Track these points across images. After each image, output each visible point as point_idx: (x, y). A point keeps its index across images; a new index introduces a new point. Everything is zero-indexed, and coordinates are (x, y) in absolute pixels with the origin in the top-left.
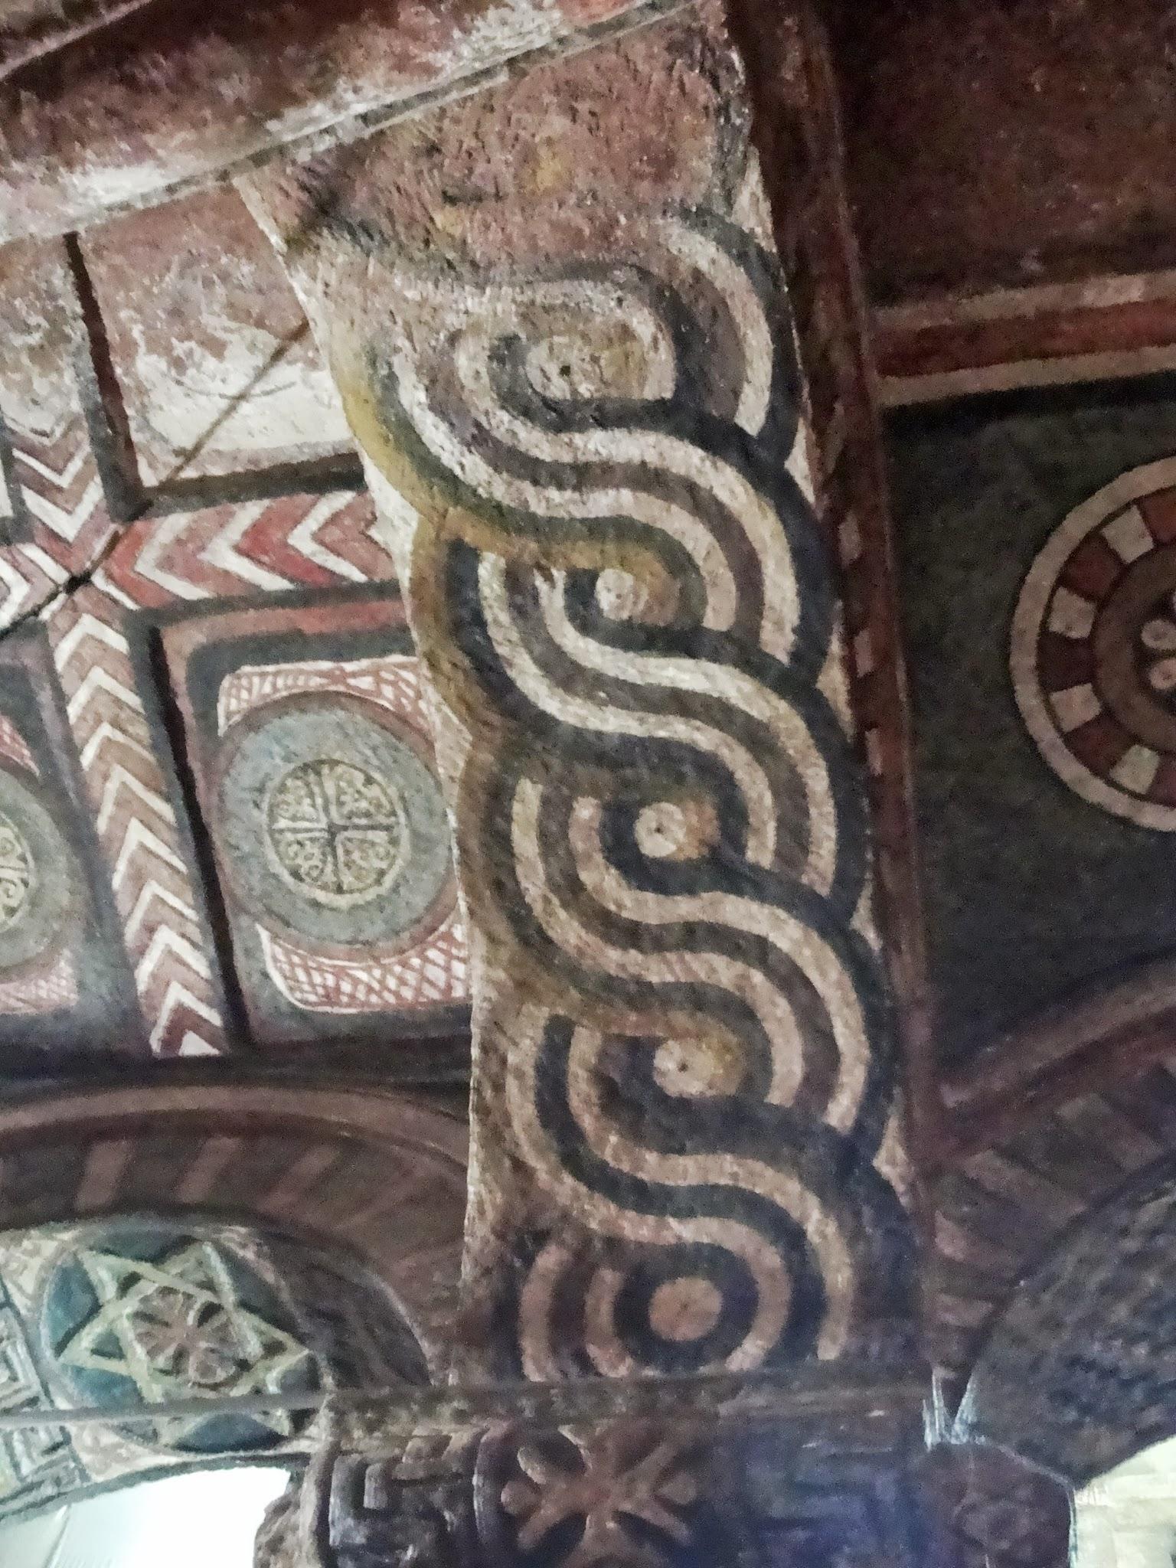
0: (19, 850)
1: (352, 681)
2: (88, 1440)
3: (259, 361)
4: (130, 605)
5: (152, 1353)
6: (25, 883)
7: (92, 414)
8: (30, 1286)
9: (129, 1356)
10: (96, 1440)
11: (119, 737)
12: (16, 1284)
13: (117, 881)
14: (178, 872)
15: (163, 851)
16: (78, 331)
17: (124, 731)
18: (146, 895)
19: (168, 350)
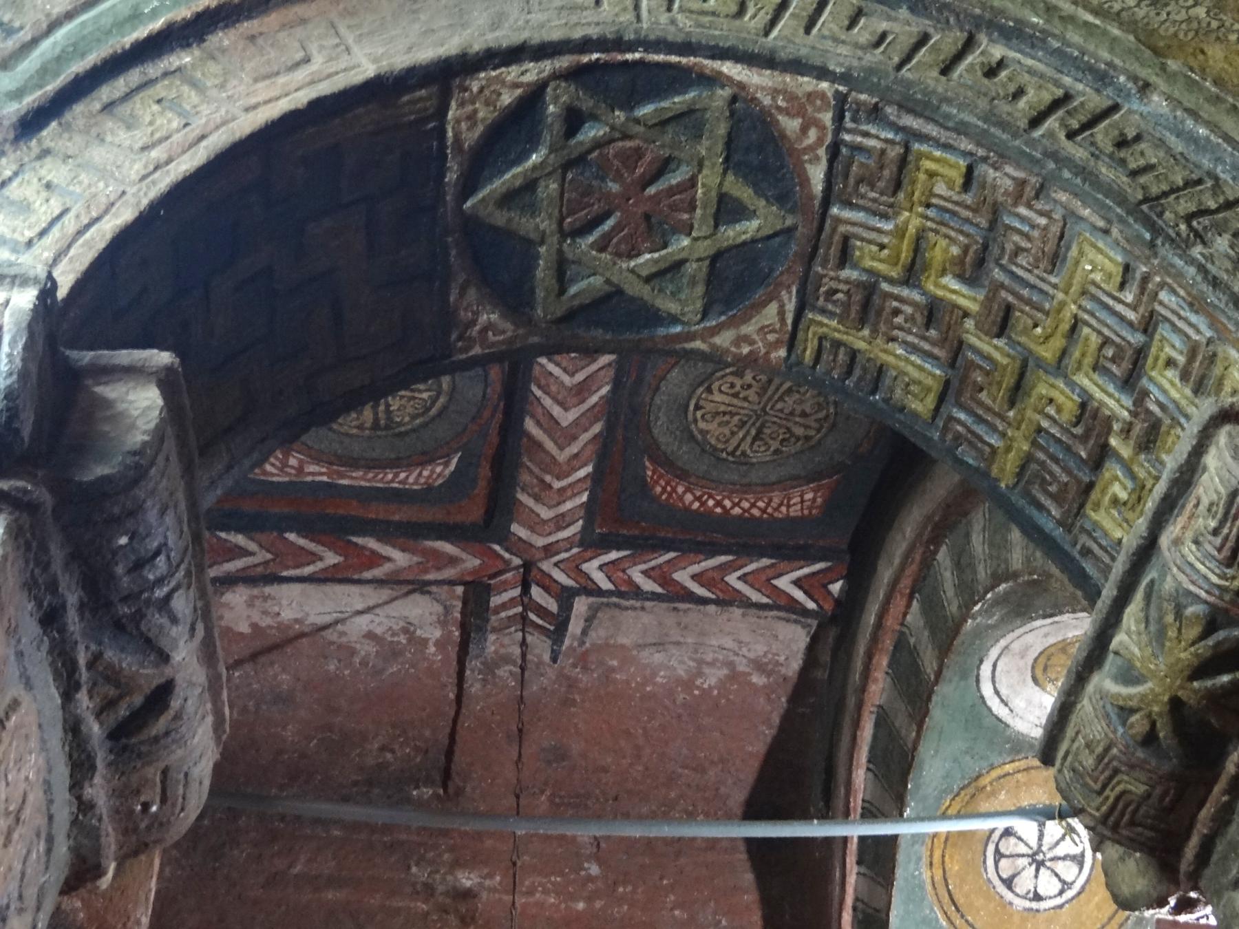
0: (699, 414)
1: (324, 470)
2: (813, 134)
3: (339, 627)
4: (497, 548)
5: (692, 183)
6: (709, 390)
7: (482, 630)
8: (773, 308)
9: (714, 194)
10: (804, 130)
11: (548, 478)
12: (783, 320)
13: (605, 390)
14: (540, 387)
15: (547, 402)
16: (473, 664)
17: (542, 481)
18: (580, 377)
19: (410, 640)
